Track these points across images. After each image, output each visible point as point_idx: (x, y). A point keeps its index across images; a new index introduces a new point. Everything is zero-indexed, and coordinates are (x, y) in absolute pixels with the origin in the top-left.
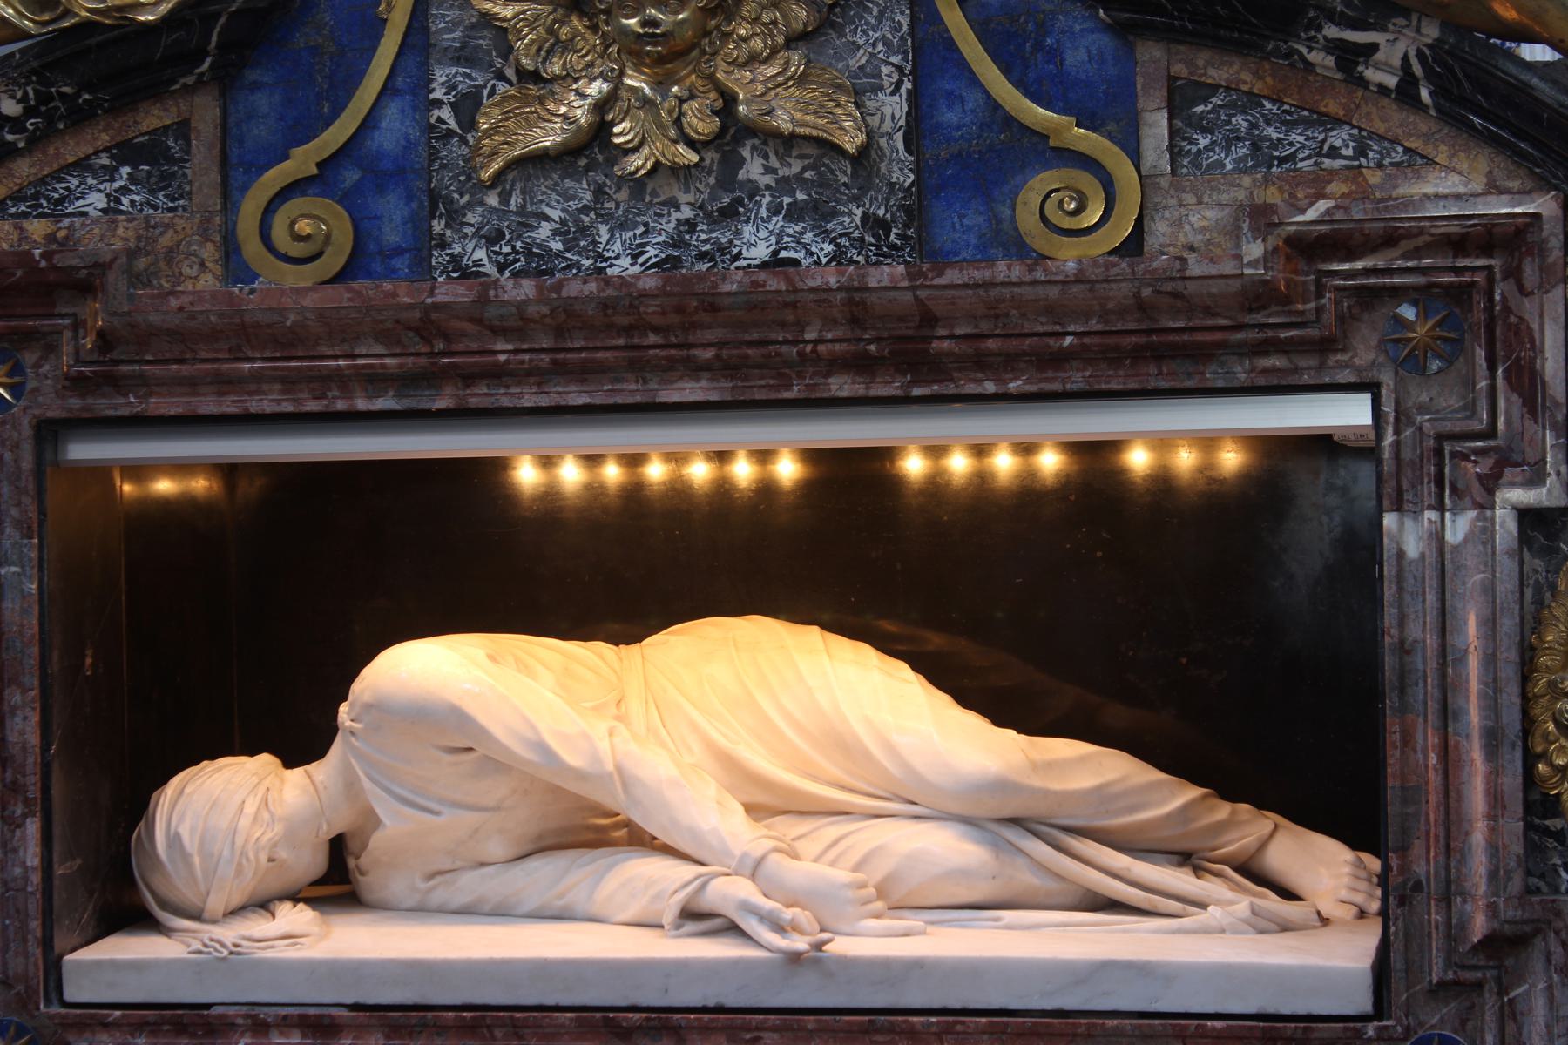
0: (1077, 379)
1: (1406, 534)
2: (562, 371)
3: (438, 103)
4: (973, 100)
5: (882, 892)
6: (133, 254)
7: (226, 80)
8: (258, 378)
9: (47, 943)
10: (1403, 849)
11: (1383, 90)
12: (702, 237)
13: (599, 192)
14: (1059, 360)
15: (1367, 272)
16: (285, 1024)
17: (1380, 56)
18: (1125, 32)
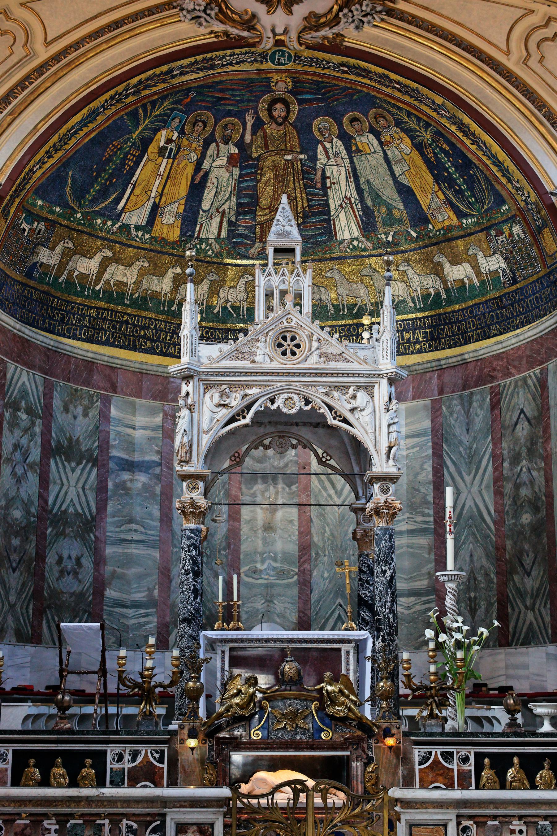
1: (354, 764)
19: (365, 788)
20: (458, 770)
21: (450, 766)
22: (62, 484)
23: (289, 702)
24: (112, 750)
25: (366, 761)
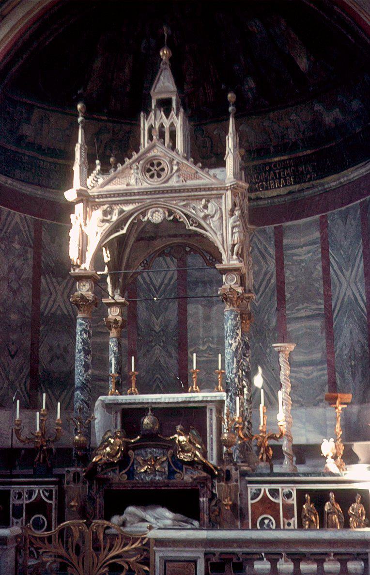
1: (201, 500)
20: (283, 505)
21: (276, 501)
22: (51, 294)
24: (14, 489)
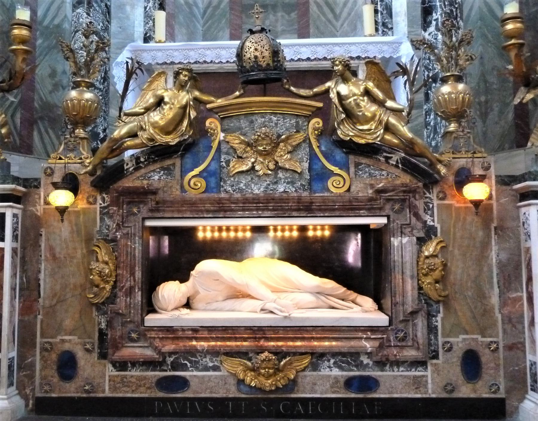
0: (337, 213)
1: (395, 242)
2: (243, 210)
3: (222, 162)
4: (320, 164)
5: (296, 304)
6: (164, 187)
7: (182, 157)
8: (186, 210)
9: (142, 315)
10: (395, 297)
11: (392, 165)
12: (271, 187)
13: (252, 179)
14: (334, 210)
15: (389, 196)
16: (188, 330)
17: (393, 159)
18: (347, 153)
19: (420, 288)
23: (260, 120)
25: (422, 234)
